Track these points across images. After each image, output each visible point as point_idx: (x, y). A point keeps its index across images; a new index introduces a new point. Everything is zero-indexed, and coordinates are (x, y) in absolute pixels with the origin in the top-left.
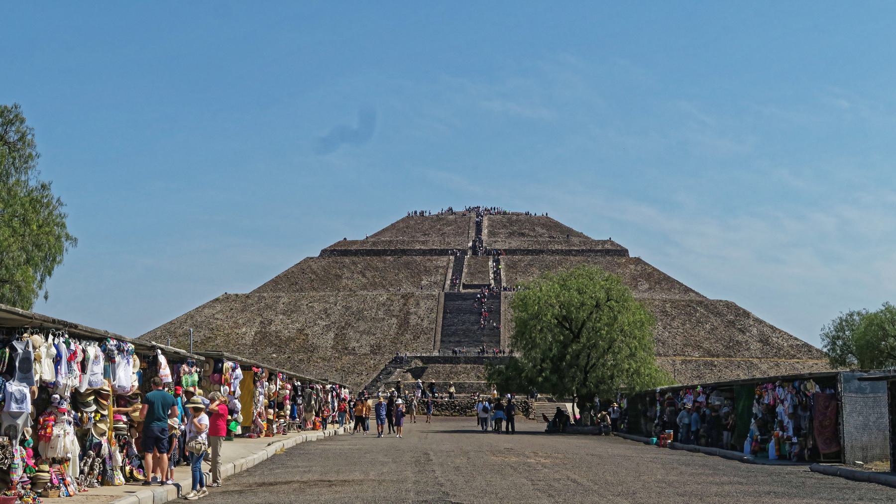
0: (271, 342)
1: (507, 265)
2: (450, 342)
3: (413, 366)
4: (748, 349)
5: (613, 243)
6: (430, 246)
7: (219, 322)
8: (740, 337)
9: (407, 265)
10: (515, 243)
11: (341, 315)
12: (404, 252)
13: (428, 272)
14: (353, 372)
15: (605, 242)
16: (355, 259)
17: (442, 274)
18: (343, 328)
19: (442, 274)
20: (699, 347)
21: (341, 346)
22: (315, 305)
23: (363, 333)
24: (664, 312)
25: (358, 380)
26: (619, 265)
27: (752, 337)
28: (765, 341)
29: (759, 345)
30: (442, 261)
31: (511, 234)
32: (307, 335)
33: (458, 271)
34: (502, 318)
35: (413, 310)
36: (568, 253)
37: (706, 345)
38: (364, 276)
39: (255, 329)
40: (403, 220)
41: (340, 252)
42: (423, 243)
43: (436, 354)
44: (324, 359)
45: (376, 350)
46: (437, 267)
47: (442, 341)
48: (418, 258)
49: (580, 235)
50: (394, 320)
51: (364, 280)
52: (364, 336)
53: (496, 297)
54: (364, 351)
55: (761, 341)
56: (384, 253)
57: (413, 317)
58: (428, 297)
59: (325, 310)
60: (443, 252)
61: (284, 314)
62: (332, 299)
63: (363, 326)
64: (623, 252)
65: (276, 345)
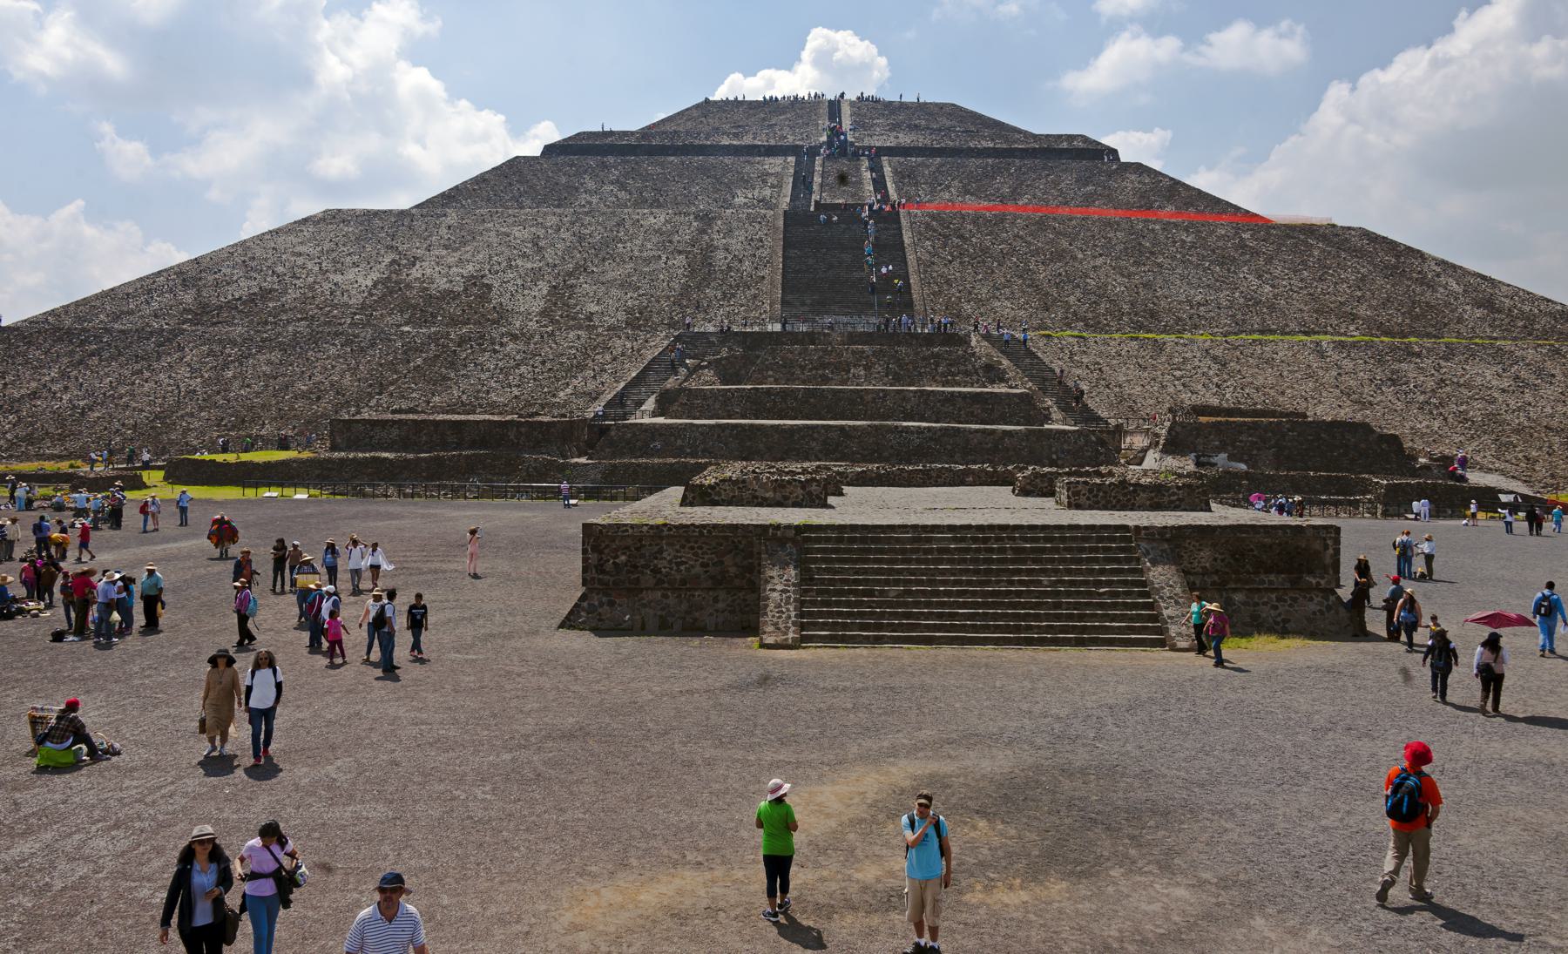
0: (405, 300)
1: (895, 172)
2: (803, 304)
3: (724, 352)
4: (1460, 320)
5: (1085, 139)
6: (747, 140)
7: (300, 261)
9: (704, 170)
10: (905, 139)
11: (569, 250)
12: (702, 150)
13: (746, 183)
14: (581, 367)
15: (1071, 138)
16: (611, 159)
17: (772, 186)
18: (570, 274)
19: (772, 186)
20: (1354, 317)
22: (517, 232)
23: (611, 283)
24: (1242, 245)
25: (591, 386)
26: (1110, 175)
27: (1452, 293)
28: (1489, 304)
29: (1479, 313)
30: (774, 164)
31: (895, 127)
32: (489, 287)
33: (802, 182)
34: (911, 258)
35: (719, 241)
36: (1011, 153)
38: (623, 187)
39: (375, 276)
40: (697, 106)
41: (581, 152)
42: (736, 135)
43: (778, 327)
44: (514, 337)
45: (638, 322)
46: (764, 177)
47: (784, 303)
48: (727, 160)
49: (1019, 131)
50: (680, 260)
51: (622, 195)
52: (614, 292)
53: (888, 218)
56: (663, 150)
57: (720, 254)
58: (752, 219)
59: (535, 241)
60: (771, 151)
61: (446, 247)
62: (552, 220)
63: (614, 272)
65: (415, 307)
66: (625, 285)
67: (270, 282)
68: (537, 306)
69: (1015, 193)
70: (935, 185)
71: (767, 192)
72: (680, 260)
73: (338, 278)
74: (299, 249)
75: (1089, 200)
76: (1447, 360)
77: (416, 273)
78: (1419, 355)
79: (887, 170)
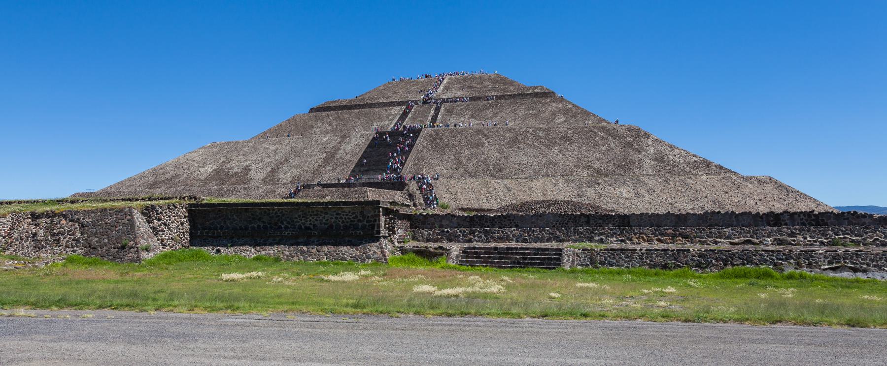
8: (634, 157)
13: (380, 119)
20: (589, 167)
21: (272, 179)
31: (462, 88)
32: (250, 170)
37: (597, 165)
54: (285, 181)
55: (656, 159)
64: (547, 94)
66: (296, 167)
67: (179, 171)
68: (262, 176)
69: (494, 115)
70: (461, 114)
71: (387, 122)
72: (325, 155)
73: (201, 169)
74: (197, 159)
75: (526, 116)
76: (610, 185)
77: (228, 166)
78: (599, 184)
79: (443, 109)
